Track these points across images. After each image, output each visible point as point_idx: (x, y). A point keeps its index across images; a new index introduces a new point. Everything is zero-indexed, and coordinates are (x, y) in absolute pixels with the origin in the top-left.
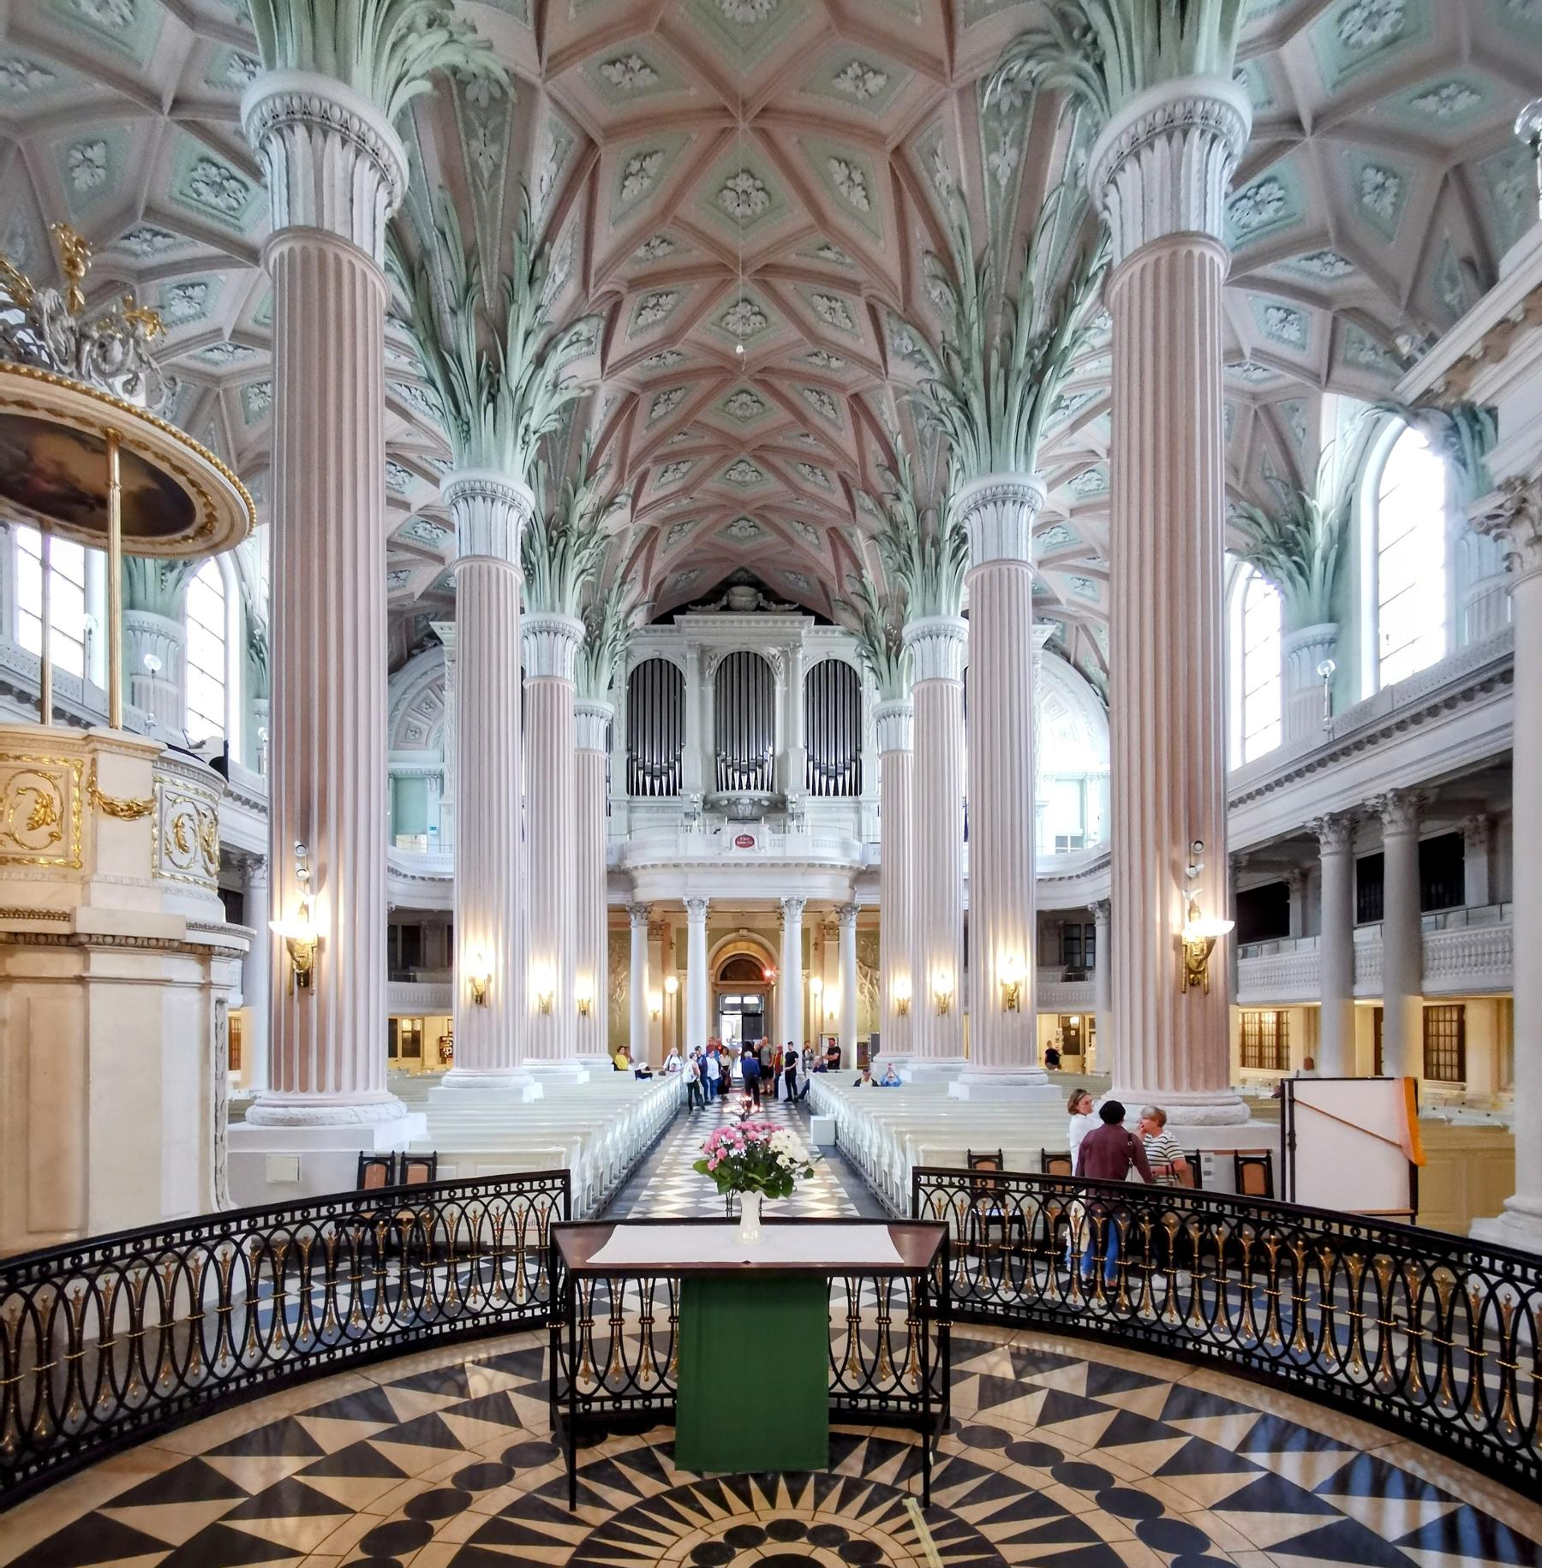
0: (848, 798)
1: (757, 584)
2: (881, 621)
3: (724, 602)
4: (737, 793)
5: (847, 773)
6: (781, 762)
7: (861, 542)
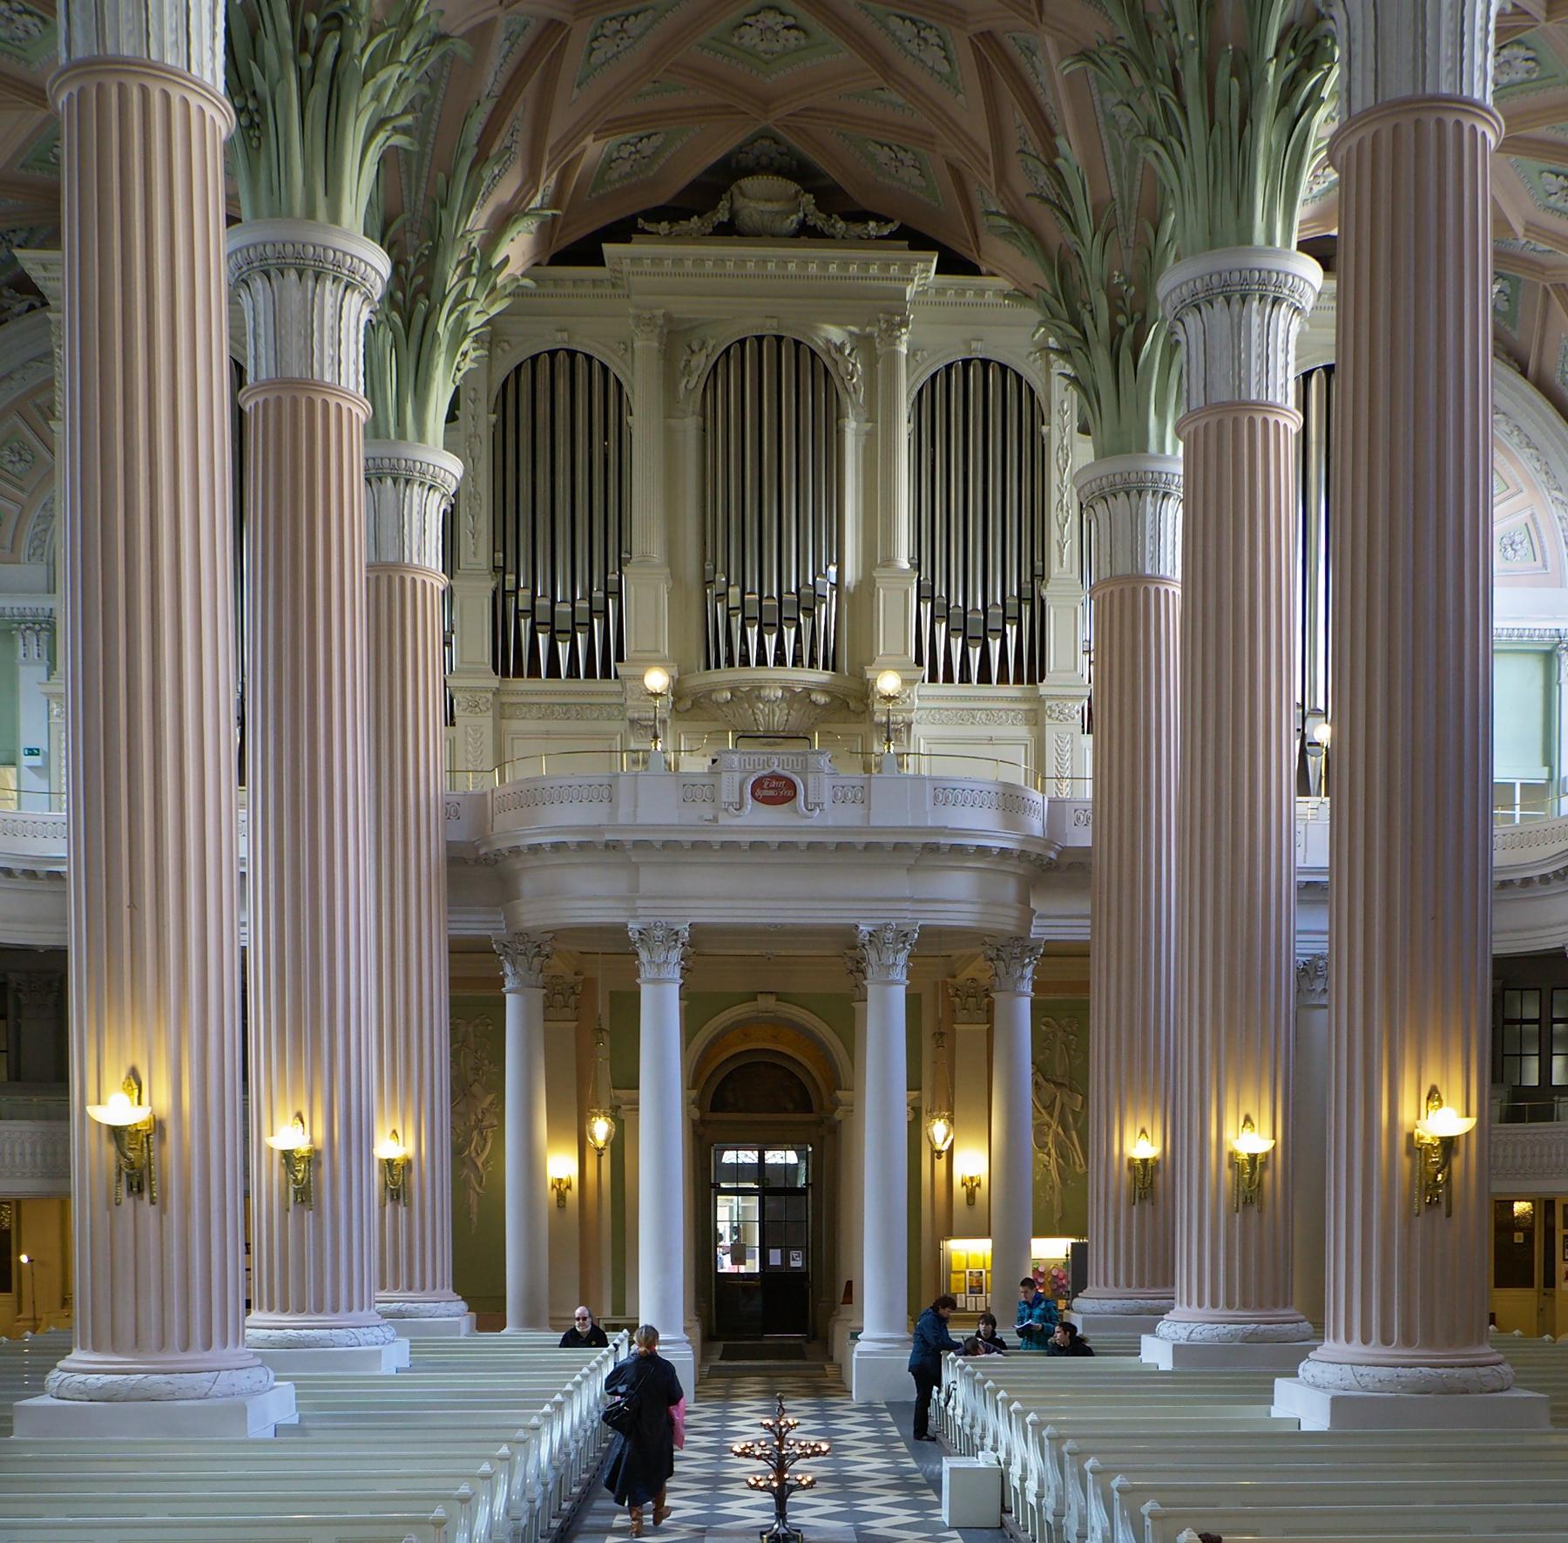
0: (1012, 690)
1: (801, 173)
2: (1095, 263)
3: (723, 216)
4: (754, 673)
5: (1011, 631)
6: (858, 603)
7: (1054, 72)
